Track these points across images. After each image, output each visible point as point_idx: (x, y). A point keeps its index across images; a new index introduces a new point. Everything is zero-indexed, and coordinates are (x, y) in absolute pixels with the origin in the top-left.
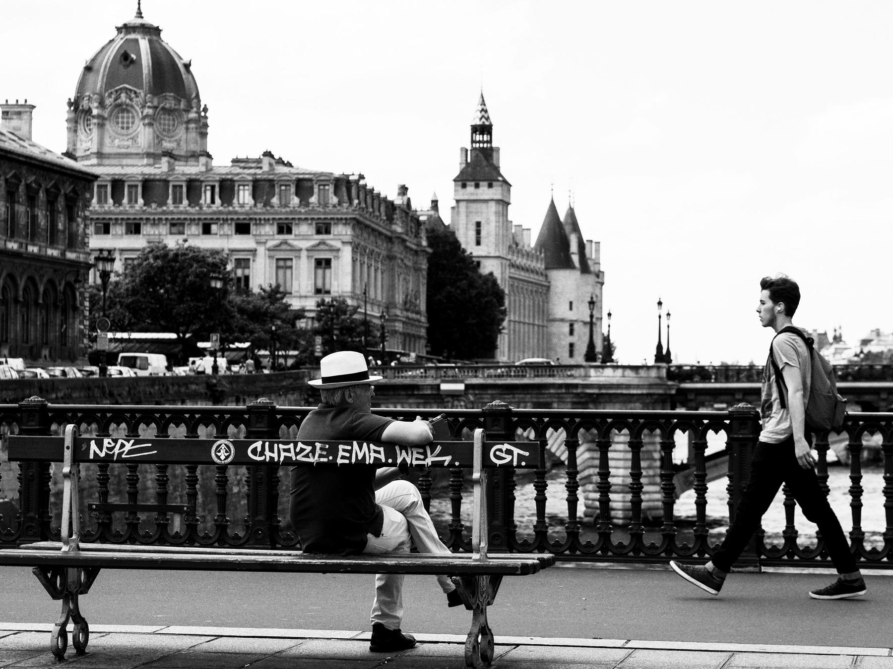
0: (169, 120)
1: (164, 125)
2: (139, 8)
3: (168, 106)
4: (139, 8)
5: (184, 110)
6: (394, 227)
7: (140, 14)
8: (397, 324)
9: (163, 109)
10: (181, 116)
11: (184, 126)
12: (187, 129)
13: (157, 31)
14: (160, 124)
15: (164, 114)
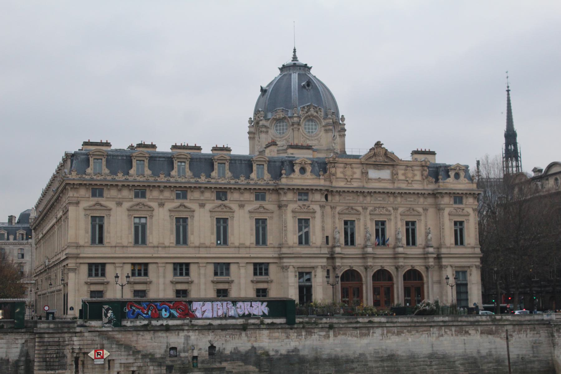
0: (283, 126)
1: (280, 130)
2: (295, 55)
3: (278, 117)
4: (295, 55)
5: (290, 117)
6: (284, 181)
7: (295, 58)
8: (285, 260)
9: (274, 119)
10: (288, 121)
11: (291, 127)
12: (293, 129)
13: (306, 68)
14: (277, 130)
15: (280, 122)
